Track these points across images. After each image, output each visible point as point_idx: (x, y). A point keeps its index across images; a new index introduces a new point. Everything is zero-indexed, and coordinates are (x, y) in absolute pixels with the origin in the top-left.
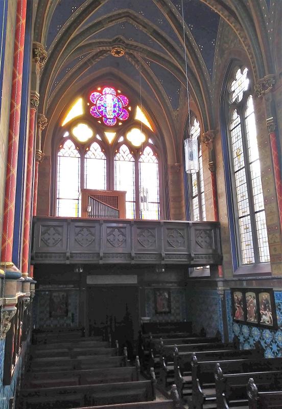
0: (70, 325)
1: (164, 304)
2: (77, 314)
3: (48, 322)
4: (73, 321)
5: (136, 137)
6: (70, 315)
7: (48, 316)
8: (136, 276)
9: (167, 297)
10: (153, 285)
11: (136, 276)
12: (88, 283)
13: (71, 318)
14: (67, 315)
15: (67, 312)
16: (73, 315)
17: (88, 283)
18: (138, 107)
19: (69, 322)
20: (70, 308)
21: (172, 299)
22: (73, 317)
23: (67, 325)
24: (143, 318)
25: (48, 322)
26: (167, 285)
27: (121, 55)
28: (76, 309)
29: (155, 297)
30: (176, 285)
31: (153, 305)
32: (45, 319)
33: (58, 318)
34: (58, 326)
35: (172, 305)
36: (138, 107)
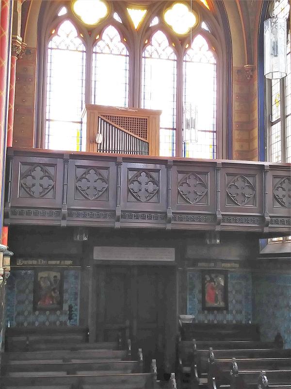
0: (65, 323)
1: (216, 296)
2: (78, 307)
4: (70, 318)
6: (66, 307)
8: (173, 250)
9: (222, 284)
10: (200, 264)
11: (173, 250)
14: (61, 308)
15: (60, 303)
16: (70, 307)
17: (95, 258)
19: (64, 318)
20: (66, 296)
24: (182, 316)
25: (31, 318)
26: (223, 265)
31: (200, 296)
32: (26, 313)
33: (48, 313)
34: (47, 323)
35: (231, 297)
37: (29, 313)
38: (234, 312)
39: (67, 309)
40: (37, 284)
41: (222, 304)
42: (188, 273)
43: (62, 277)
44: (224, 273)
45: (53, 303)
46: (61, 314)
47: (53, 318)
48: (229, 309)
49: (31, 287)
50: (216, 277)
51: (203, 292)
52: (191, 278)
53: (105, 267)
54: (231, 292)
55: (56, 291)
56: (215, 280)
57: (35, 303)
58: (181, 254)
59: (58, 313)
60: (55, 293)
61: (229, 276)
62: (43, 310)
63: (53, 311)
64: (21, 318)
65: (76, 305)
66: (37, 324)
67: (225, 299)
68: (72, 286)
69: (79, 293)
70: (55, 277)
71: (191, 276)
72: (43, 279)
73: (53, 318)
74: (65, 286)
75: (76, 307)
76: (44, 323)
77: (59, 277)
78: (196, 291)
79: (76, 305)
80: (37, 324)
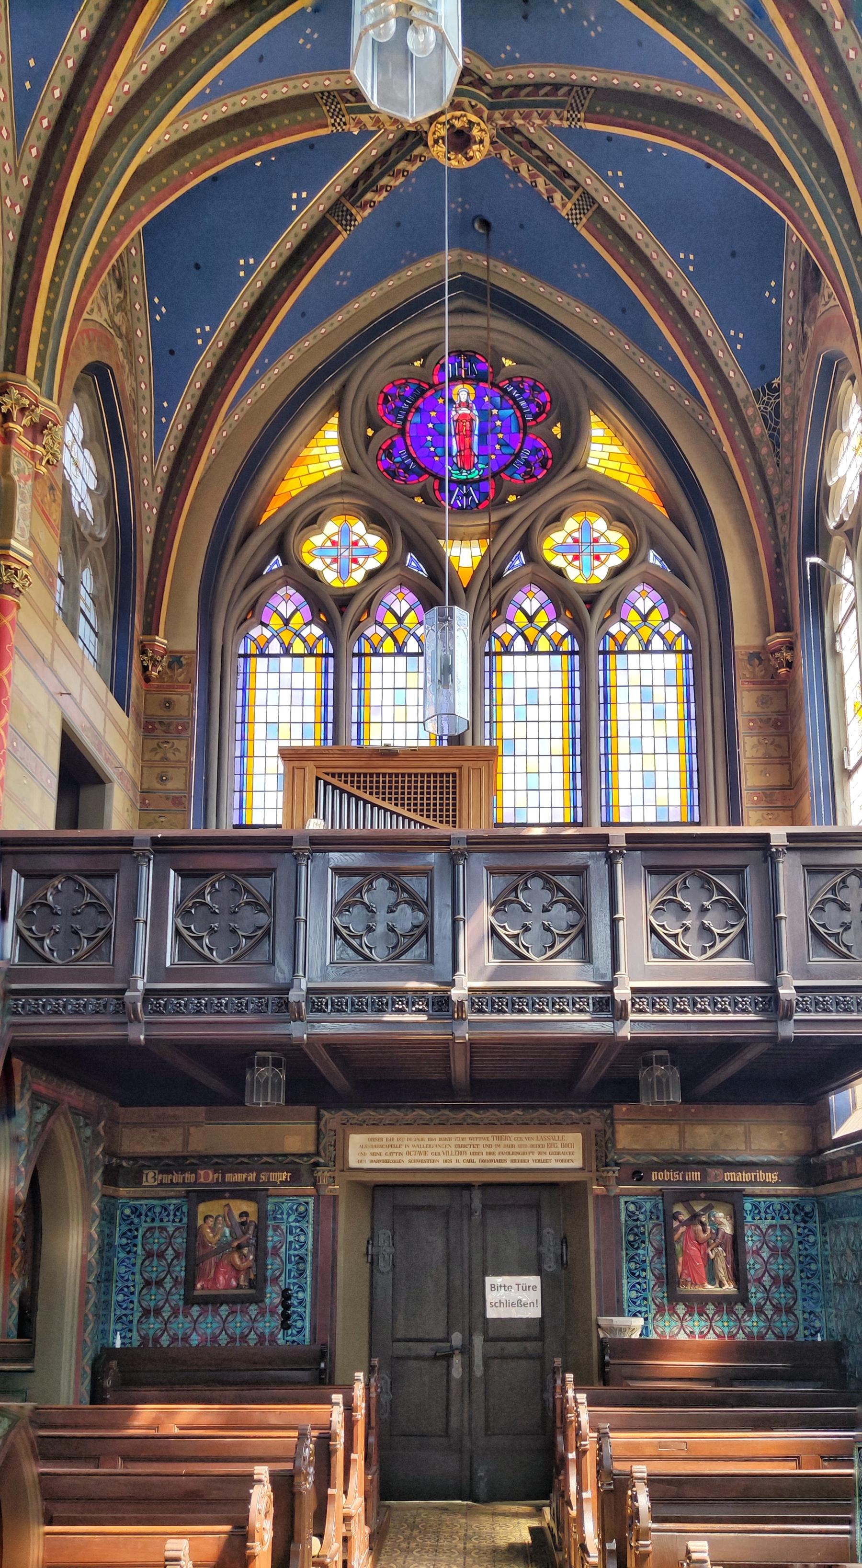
0: (273, 1339)
1: (711, 1264)
2: (307, 1296)
3: (180, 1325)
4: (285, 1325)
5: (585, 547)
6: (273, 1296)
7: (177, 1298)
8: (575, 1139)
9: (727, 1229)
10: (654, 1176)
11: (575, 1139)
12: (353, 1162)
13: (280, 1309)
14: (258, 1299)
15: (258, 1283)
16: (286, 1295)
17: (353, 1162)
18: (594, 418)
19: (269, 1324)
20: (273, 1265)
21: (751, 1242)
22: (286, 1307)
23: (261, 1337)
24: (603, 1321)
25: (180, 1325)
26: (730, 1176)
27: (478, 153)
28: (301, 1273)
29: (668, 1232)
30: (772, 1177)
31: (660, 1265)
32: (166, 1315)
33: (224, 1310)
34: (223, 1339)
35: (753, 1265)
36: (594, 418)
37: (175, 1312)
38: (769, 1310)
39: (277, 1301)
40: (193, 1232)
41: (729, 1288)
42: (623, 1200)
43: (263, 1215)
44: (732, 1199)
45: (239, 1287)
46: (262, 1313)
47: (238, 1324)
48: (753, 1301)
49: (180, 1241)
50: (709, 1208)
51: (668, 1251)
52: (630, 1215)
53: (387, 1194)
54: (757, 1252)
55: (245, 1250)
56: (704, 1219)
57: (189, 1283)
58: (600, 1151)
59: (253, 1309)
60: (243, 1257)
61: (748, 1206)
62: (212, 1302)
63: (236, 1301)
64: (153, 1325)
65: (302, 1289)
66: (195, 1340)
67: (738, 1275)
68: (291, 1238)
69: (309, 1259)
70: (244, 1214)
71: (632, 1208)
72: (210, 1222)
73: (238, 1324)
74: (272, 1238)
75: (301, 1295)
76: (214, 1338)
77: (253, 1217)
78: (647, 1252)
79: (302, 1289)
80: (195, 1340)
